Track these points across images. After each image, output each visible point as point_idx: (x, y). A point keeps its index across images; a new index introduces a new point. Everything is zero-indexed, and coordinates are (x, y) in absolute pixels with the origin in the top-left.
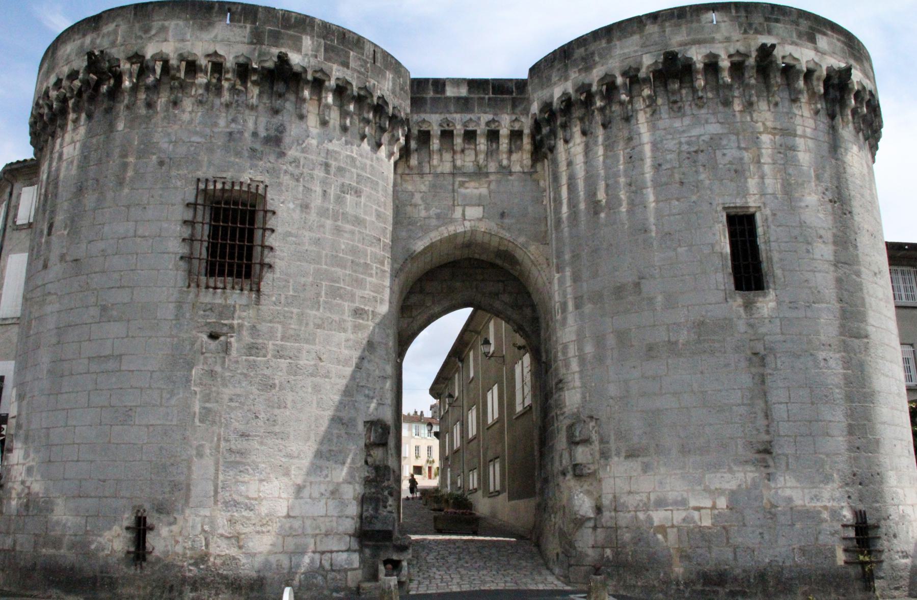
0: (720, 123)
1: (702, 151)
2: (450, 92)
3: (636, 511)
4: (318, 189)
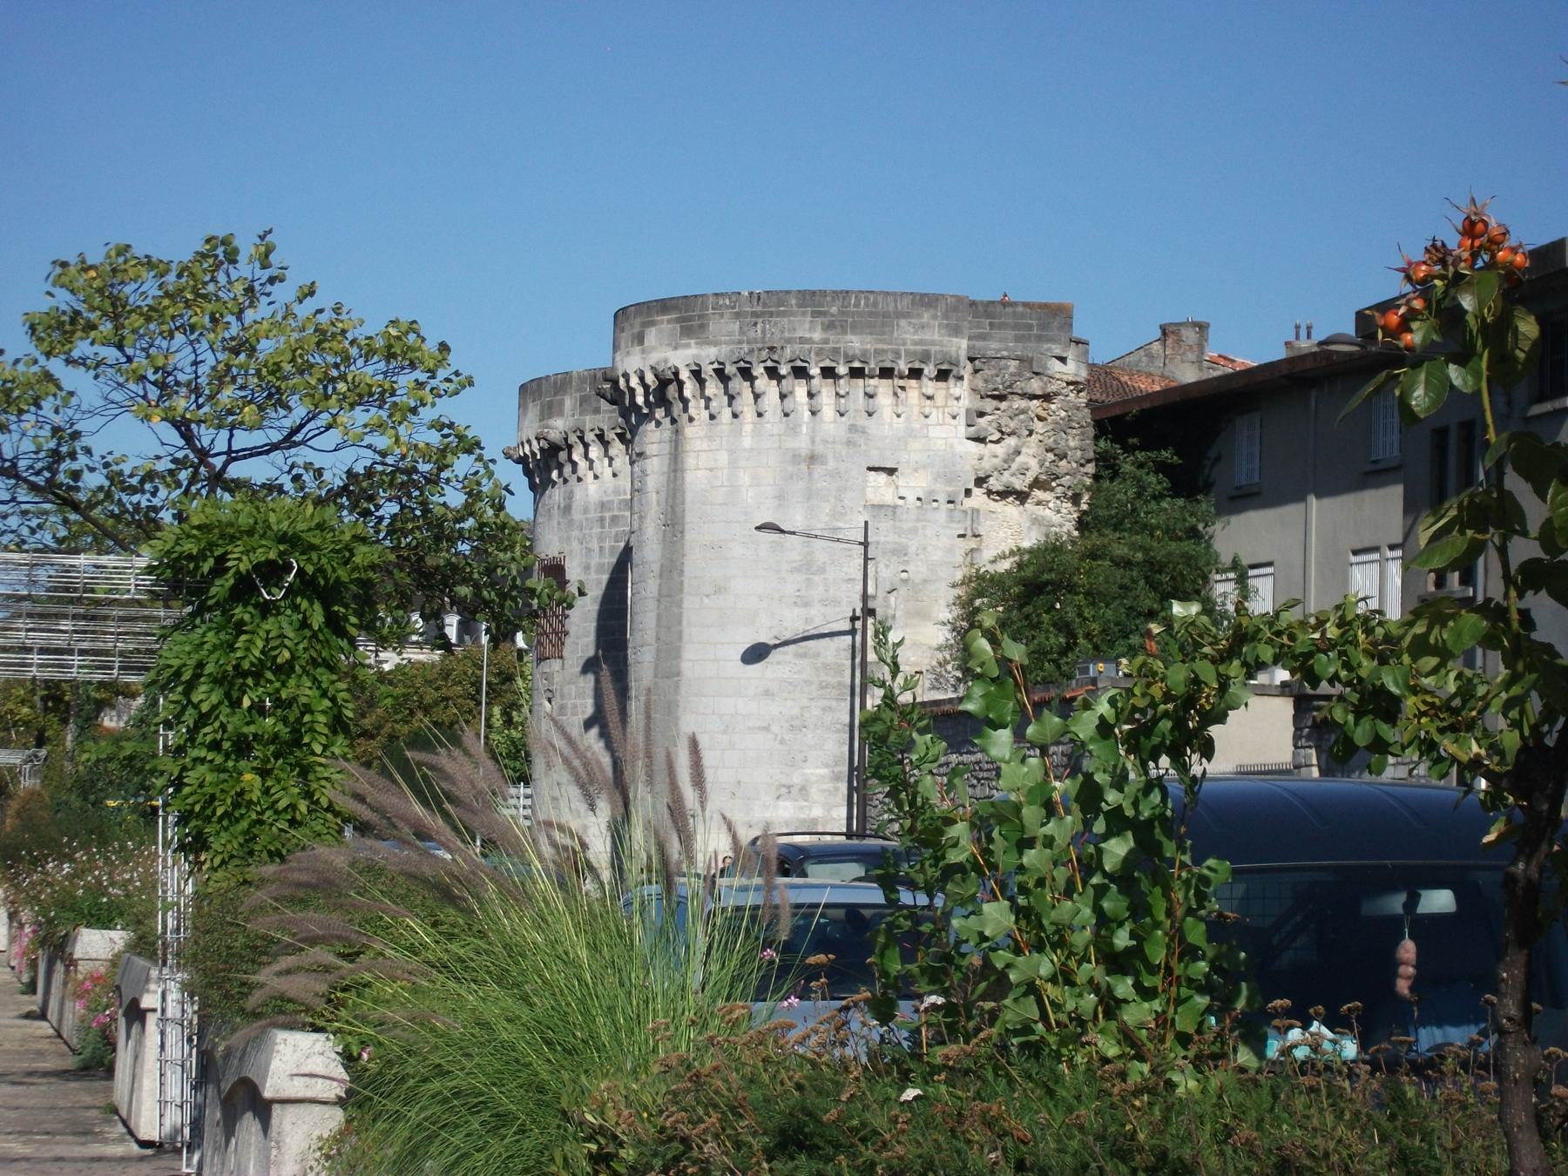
4: (595, 546)
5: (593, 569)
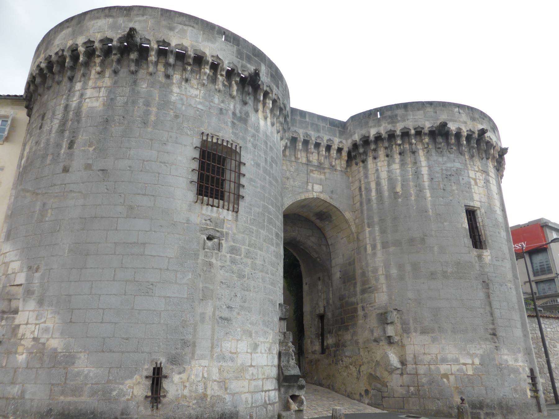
0: (461, 163)
1: (453, 175)
3: (429, 365)
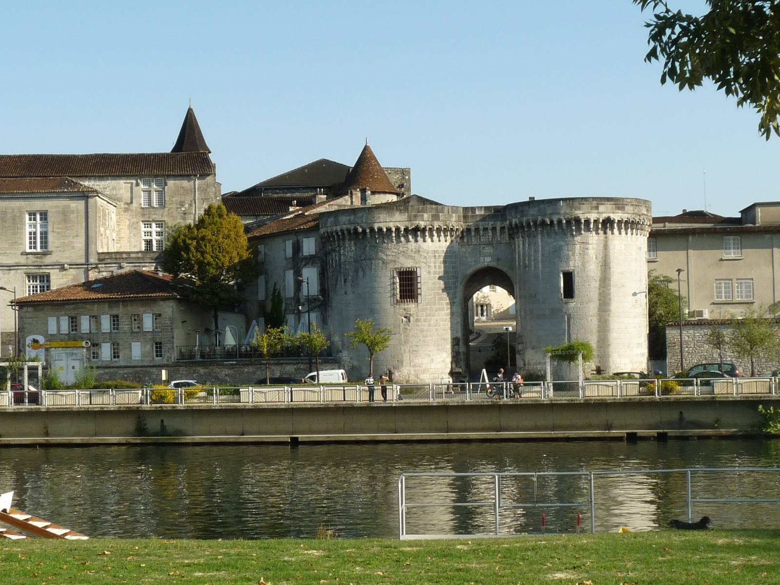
2: (477, 213)
4: (432, 265)
5: (432, 273)
